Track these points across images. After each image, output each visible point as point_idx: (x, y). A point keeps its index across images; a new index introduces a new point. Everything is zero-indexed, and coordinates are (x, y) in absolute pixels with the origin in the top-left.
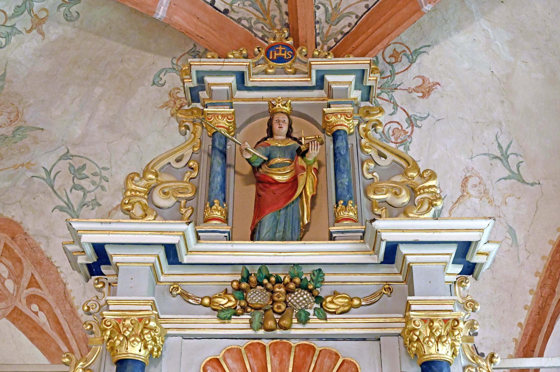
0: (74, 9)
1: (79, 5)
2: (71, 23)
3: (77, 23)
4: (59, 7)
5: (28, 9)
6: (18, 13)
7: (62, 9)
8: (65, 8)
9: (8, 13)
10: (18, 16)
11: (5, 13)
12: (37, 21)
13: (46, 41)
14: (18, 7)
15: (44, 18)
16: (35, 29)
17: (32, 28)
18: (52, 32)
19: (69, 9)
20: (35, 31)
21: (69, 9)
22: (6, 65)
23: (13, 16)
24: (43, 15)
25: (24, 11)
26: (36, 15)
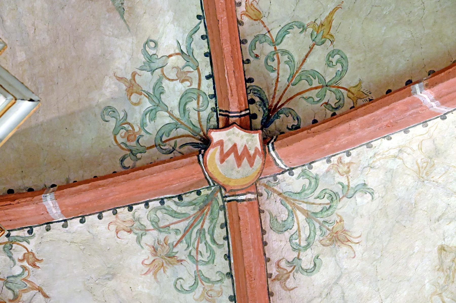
0: (112, 123)
1: (112, 130)
2: (103, 107)
3: (98, 111)
4: (126, 115)
5: (152, 96)
6: (157, 86)
7: (122, 115)
8: (121, 118)
9: (167, 81)
10: (156, 84)
11: (169, 80)
12: (135, 88)
13: (111, 73)
14: (162, 93)
15: (131, 95)
16: (130, 80)
17: (134, 80)
18: (113, 86)
19: (117, 119)
20: (129, 77)
21: (117, 119)
22: (127, 25)
23: (159, 81)
24: (134, 98)
25: (154, 92)
26: (141, 94)
